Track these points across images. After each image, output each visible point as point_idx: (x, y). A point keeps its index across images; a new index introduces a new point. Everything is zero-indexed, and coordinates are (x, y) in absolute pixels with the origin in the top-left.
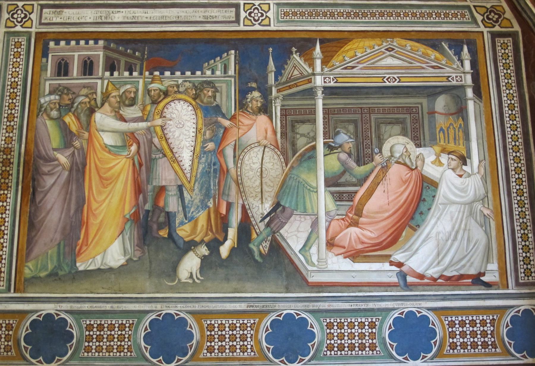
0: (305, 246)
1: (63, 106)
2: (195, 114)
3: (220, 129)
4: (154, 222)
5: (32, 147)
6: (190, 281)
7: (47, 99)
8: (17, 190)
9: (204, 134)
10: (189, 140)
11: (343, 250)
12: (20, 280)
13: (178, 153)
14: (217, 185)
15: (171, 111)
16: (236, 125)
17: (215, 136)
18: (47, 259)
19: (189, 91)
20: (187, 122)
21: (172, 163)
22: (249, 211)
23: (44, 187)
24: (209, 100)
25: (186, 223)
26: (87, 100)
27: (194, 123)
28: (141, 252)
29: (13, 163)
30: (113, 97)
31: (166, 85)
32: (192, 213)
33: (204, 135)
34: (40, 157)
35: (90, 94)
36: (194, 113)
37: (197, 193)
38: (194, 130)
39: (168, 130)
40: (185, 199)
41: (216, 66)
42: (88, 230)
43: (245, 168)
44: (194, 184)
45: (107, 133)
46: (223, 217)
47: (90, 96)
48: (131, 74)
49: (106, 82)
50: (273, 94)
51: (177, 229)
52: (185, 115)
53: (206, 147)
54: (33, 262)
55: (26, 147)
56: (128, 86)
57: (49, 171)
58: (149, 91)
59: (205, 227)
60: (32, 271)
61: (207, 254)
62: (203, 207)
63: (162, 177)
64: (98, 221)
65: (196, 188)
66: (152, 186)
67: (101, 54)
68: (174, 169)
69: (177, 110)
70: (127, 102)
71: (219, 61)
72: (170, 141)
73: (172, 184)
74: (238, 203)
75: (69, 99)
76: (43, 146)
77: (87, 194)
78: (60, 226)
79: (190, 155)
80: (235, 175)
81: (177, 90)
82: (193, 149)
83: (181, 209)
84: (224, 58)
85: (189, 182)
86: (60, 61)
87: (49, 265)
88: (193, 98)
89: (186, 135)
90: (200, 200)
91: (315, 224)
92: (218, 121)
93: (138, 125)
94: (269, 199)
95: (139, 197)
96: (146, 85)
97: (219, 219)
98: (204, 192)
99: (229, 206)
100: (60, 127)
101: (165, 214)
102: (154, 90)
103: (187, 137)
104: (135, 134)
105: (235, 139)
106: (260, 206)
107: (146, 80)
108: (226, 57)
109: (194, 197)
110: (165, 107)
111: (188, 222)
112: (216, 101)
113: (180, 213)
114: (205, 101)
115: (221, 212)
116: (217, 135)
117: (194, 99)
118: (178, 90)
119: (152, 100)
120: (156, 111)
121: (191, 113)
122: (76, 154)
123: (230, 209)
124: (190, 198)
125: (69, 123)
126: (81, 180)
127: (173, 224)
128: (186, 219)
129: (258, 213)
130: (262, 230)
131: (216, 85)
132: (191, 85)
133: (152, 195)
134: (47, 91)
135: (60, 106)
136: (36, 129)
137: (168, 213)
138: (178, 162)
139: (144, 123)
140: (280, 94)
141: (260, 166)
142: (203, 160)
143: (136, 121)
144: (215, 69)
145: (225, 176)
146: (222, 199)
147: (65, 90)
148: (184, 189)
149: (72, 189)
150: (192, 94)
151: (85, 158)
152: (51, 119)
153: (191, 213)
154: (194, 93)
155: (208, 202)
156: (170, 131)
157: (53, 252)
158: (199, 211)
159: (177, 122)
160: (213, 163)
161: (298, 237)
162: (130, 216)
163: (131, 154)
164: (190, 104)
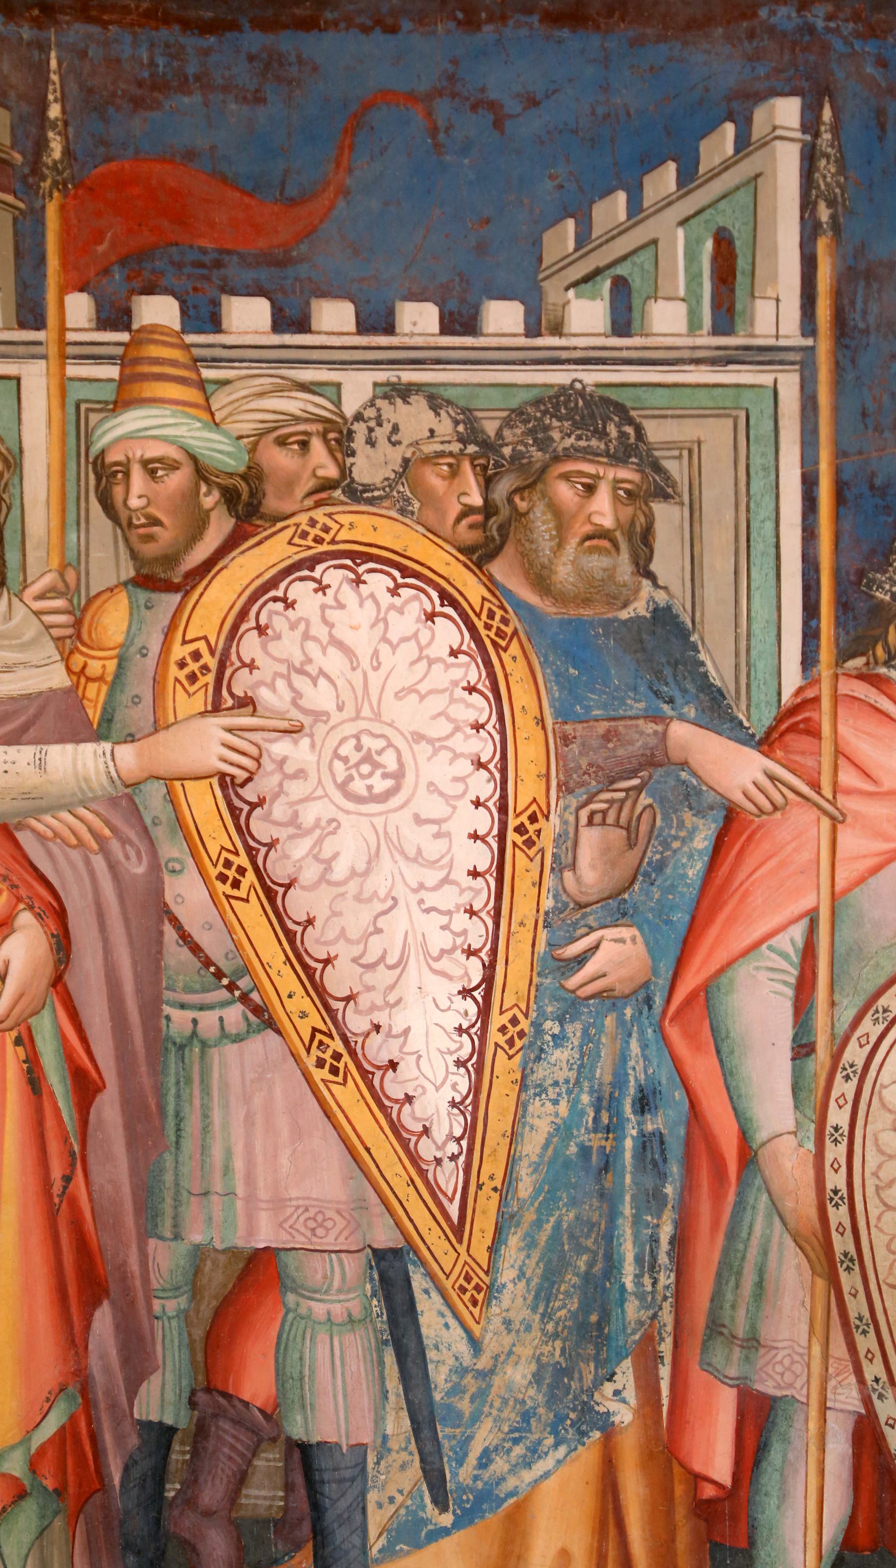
2: (484, 686)
3: (689, 818)
4: (208, 1514)
10: (448, 898)
13: (364, 1001)
14: (663, 1259)
15: (298, 658)
16: (816, 786)
19: (434, 479)
20: (424, 749)
21: (320, 1075)
24: (597, 563)
25: (445, 1532)
27: (480, 765)
32: (485, 1460)
33: (558, 868)
36: (474, 674)
37: (520, 1313)
38: (483, 821)
39: (279, 811)
40: (431, 1355)
41: (644, 257)
44: (493, 1250)
46: (710, 1502)
52: (411, 690)
53: (581, 960)
62: (560, 1419)
63: (250, 1179)
65: (507, 1275)
66: (182, 1248)
68: (336, 1126)
69: (340, 645)
71: (668, 203)
73: (329, 1242)
74: (824, 1408)
79: (453, 1020)
80: (809, 1197)
81: (332, 472)
82: (477, 977)
84: (715, 174)
85: (458, 1230)
88: (466, 550)
89: (418, 858)
90: (541, 1366)
92: (675, 754)
93: (41, 764)
95: (87, 1327)
97: (681, 1512)
101: (288, 1457)
102: (150, 467)
103: (432, 877)
104: (23, 837)
105: (807, 902)
107: (72, 370)
108: (727, 166)
109: (492, 1344)
110: (243, 615)
111: (457, 1525)
112: (651, 576)
113: (396, 1458)
115: (697, 1467)
116: (660, 867)
118: (345, 471)
119: (134, 555)
120: (179, 651)
121: (457, 674)
123: (762, 1448)
124: (463, 1348)
127: (340, 1535)
128: (441, 1502)
131: (655, 431)
132: (445, 426)
133: (185, 1316)
138: (365, 1074)
139: (88, 749)
143: (25, 728)
144: (636, 282)
145: (731, 1198)
146: (707, 1367)
148: (418, 1282)
150: (455, 509)
153: (472, 1459)
154: (476, 500)
155: (597, 1384)
156: (294, 821)
158: (535, 1452)
159: (347, 749)
160: (632, 1089)
162: (34, 1465)
164: (445, 596)
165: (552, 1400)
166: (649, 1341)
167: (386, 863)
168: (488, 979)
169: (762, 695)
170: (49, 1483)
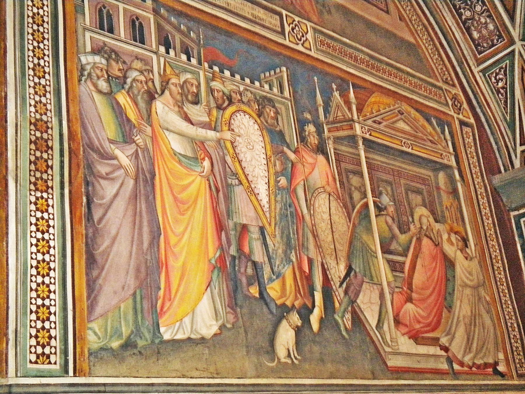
0: (379, 321)
1: (112, 77)
5: (77, 128)
6: (289, 361)
7: (91, 59)
8: (62, 195)
9: (275, 165)
11: (406, 330)
12: (82, 352)
17: (285, 169)
18: (120, 318)
22: (328, 272)
23: (103, 198)
26: (142, 78)
28: (234, 316)
29: (52, 148)
30: (173, 84)
31: (229, 88)
34: (91, 146)
35: (145, 70)
38: (265, 156)
42: (168, 275)
43: (318, 217)
45: (172, 134)
47: (146, 74)
48: (189, 59)
49: (162, 60)
50: (326, 133)
51: (267, 287)
54: (100, 321)
55: (69, 127)
56: (189, 76)
57: (107, 174)
58: (211, 91)
59: (293, 288)
60: (99, 338)
61: (299, 324)
64: (180, 263)
65: (277, 233)
67: (152, 17)
70: (190, 97)
72: (244, 164)
75: (119, 70)
76: (94, 131)
77: (160, 219)
78: (133, 263)
83: (266, 259)
86: (101, 7)
87: (124, 329)
91: (382, 296)
94: (342, 259)
95: (221, 234)
96: (208, 81)
98: (285, 240)
99: (310, 261)
100: (113, 108)
103: (260, 164)
106: (336, 267)
109: (277, 245)
114: (269, 121)
117: (259, 116)
122: (140, 155)
124: (273, 245)
125: (124, 105)
126: (151, 197)
129: (336, 275)
130: (342, 298)
134: (89, 49)
135: (109, 76)
136: (80, 102)
137: (254, 264)
140: (331, 134)
141: (329, 218)
142: (279, 198)
147: (113, 53)
149: (141, 208)
151: (153, 165)
152: (100, 92)
157: (127, 306)
161: (372, 310)
162: (216, 262)
163: (205, 171)
164: (256, 121)
165: (285, 256)
166: (295, 247)
167: (254, 160)
168: (269, 182)
169: (293, 147)
170: (219, 266)
